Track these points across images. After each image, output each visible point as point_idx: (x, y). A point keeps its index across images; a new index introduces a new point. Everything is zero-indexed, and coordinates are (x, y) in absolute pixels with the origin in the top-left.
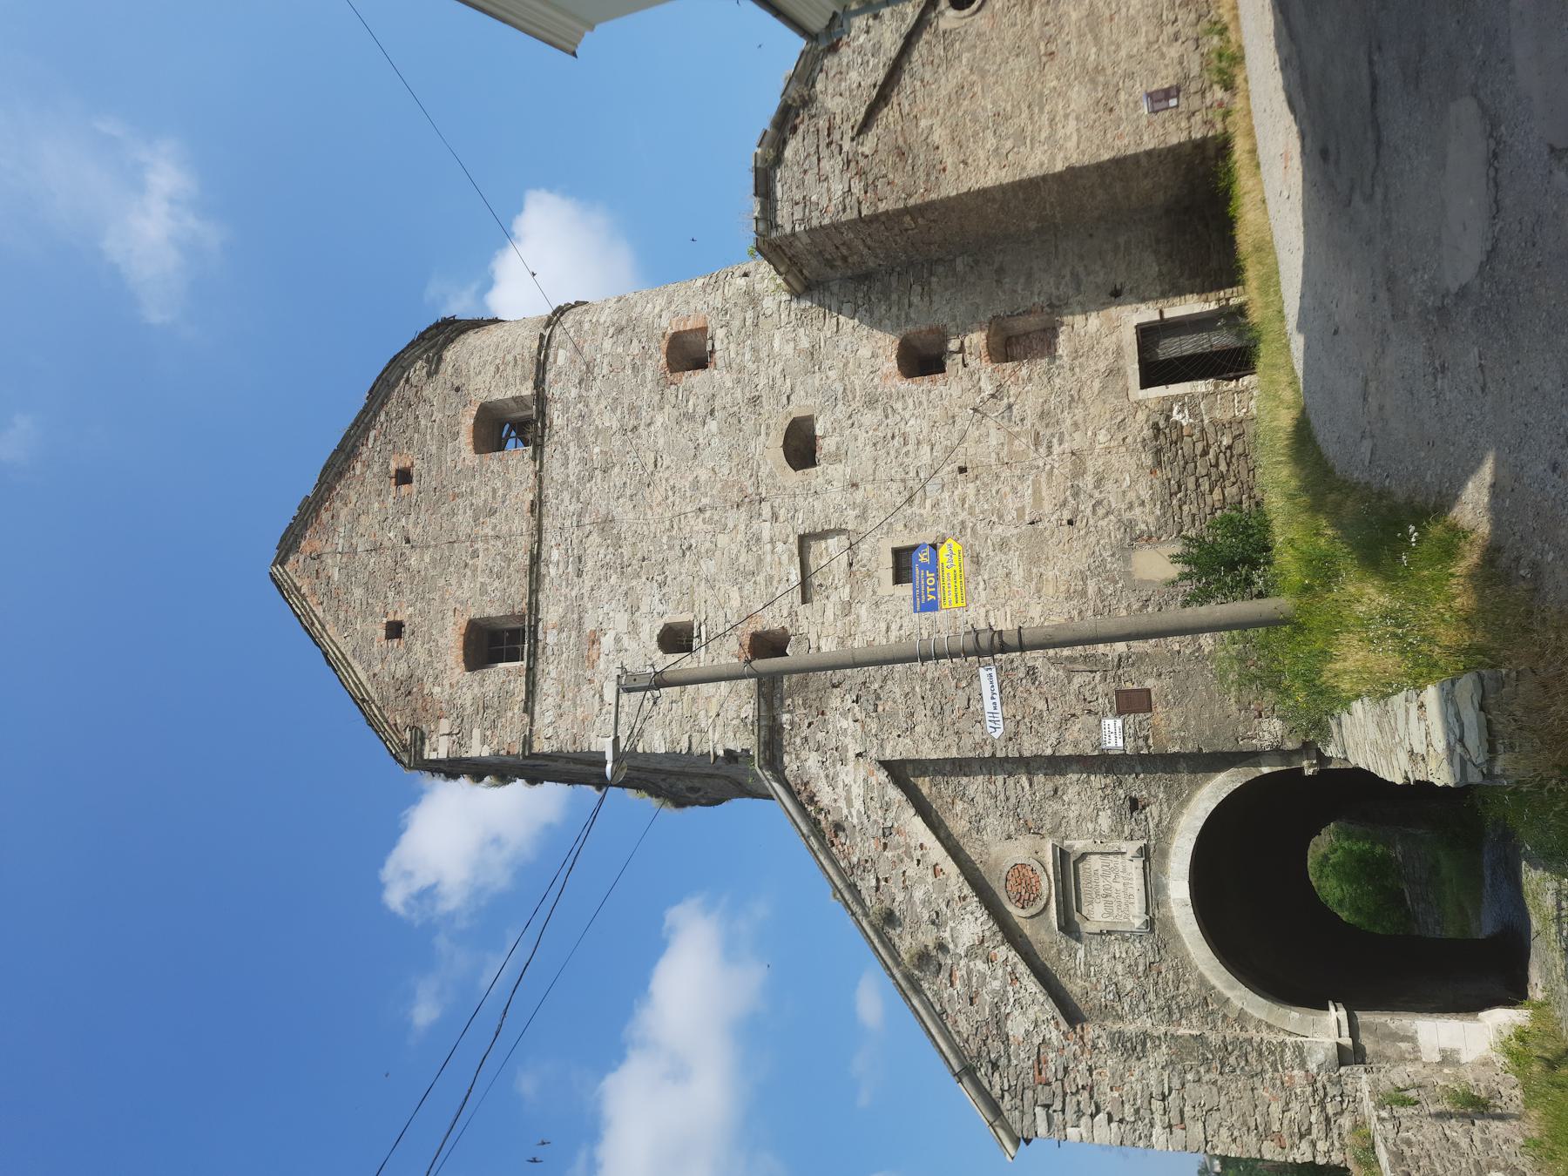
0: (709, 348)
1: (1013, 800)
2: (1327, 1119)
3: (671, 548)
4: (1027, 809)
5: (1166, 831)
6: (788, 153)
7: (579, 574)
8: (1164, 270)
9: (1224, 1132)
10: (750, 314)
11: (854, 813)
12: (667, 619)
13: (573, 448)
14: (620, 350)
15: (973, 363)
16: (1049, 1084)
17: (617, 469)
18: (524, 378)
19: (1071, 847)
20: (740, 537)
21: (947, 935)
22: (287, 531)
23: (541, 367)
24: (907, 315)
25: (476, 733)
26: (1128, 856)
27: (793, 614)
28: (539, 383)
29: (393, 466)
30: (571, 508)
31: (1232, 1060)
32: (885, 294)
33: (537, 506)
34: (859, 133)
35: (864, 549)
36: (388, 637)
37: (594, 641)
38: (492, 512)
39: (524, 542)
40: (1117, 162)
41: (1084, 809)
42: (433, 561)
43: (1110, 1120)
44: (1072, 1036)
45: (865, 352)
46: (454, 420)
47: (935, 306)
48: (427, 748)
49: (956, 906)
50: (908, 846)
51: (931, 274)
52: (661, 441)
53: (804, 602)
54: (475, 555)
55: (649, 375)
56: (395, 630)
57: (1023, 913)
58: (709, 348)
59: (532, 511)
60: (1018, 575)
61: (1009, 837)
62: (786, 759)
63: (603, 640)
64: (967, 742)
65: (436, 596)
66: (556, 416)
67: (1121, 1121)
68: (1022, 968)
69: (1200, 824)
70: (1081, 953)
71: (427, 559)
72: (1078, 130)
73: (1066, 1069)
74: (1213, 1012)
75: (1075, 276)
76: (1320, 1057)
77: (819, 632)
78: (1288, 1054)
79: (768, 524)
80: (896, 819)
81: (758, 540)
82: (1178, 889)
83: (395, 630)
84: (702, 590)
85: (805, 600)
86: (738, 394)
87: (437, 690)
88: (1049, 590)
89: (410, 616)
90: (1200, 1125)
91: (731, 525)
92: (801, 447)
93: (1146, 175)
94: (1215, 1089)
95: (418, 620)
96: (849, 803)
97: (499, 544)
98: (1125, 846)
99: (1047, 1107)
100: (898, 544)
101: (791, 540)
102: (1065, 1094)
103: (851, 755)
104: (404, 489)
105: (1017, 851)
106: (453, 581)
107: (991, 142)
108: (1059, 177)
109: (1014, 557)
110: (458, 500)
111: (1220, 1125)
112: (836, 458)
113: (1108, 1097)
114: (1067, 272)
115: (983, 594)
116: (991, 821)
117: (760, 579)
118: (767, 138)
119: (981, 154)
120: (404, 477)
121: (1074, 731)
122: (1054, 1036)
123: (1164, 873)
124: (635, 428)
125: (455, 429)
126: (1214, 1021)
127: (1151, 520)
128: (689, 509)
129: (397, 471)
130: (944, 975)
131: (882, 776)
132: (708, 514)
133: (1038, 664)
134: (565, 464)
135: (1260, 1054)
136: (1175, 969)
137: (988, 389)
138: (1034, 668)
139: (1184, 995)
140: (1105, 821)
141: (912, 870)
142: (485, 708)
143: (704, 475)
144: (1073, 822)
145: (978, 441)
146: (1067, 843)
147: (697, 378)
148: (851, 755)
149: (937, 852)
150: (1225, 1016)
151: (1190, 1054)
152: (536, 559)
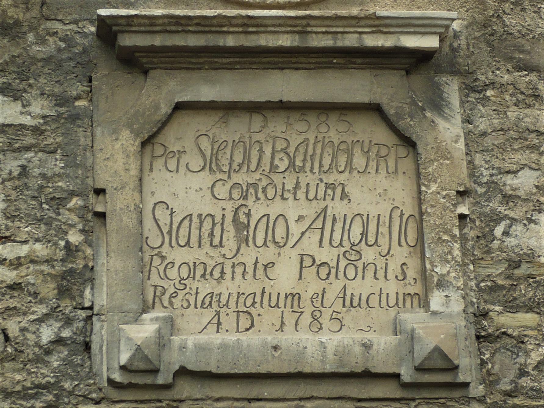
19: (438, 104)
26: (413, 319)
146: (452, 90)
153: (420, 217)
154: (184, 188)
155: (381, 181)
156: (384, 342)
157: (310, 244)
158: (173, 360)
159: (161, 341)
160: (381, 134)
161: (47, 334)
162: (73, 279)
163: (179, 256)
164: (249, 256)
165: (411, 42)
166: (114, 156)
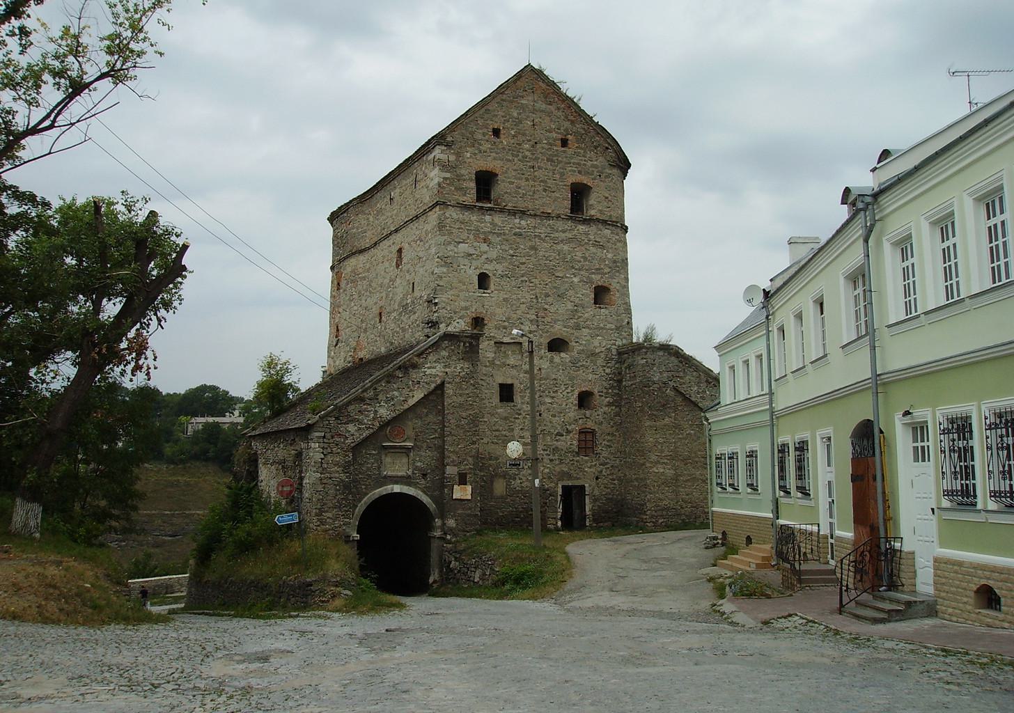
1: (427, 431)
2: (326, 531)
5: (415, 485)
6: (673, 358)
7: (515, 234)
8: (602, 497)
9: (321, 497)
10: (614, 327)
11: (426, 370)
15: (580, 421)
17: (557, 257)
21: (382, 404)
23: (604, 222)
24: (602, 396)
25: (448, 175)
28: (598, 220)
29: (569, 137)
30: (542, 231)
32: (612, 387)
33: (548, 216)
34: (675, 389)
35: (514, 372)
37: (485, 241)
38: (545, 190)
40: (646, 486)
41: (425, 458)
43: (322, 459)
44: (350, 448)
45: (590, 377)
46: (587, 173)
47: (604, 408)
48: (443, 148)
49: (392, 408)
50: (414, 391)
51: (616, 407)
52: (566, 280)
53: (495, 343)
54: (527, 180)
57: (388, 432)
58: (602, 306)
59: (543, 212)
60: (497, 433)
62: (446, 342)
66: (582, 228)
67: (322, 463)
68: (372, 431)
69: (419, 498)
70: (374, 452)
71: (527, 153)
72: (658, 472)
73: (337, 445)
75: (607, 463)
78: (346, 520)
80: (423, 386)
81: (522, 323)
82: (397, 488)
83: (496, 132)
84: (503, 295)
85: (495, 343)
87: (468, 155)
88: (493, 446)
89: (502, 142)
92: (557, 345)
93: (638, 494)
95: (500, 146)
96: (429, 368)
97: (531, 193)
99: (324, 437)
100: (515, 386)
102: (330, 443)
103: (447, 370)
105: (409, 432)
106: (515, 167)
107: (661, 440)
108: (643, 464)
109: (504, 433)
112: (551, 362)
113: (329, 458)
114: (608, 460)
118: (680, 351)
119: (658, 436)
120: (564, 143)
122: (348, 441)
123: (402, 484)
124: (573, 267)
127: (515, 486)
128: (538, 291)
130: (368, 401)
131: (439, 382)
132: (534, 300)
134: (564, 231)
135: (347, 511)
136: (370, 485)
137: (570, 428)
140: (419, 464)
141: (405, 391)
143: (550, 299)
145: (551, 422)
148: (447, 370)
149: (411, 402)
152: (523, 213)
154: (388, 460)
156: (405, 474)
162: (379, 468)
166: (383, 457)
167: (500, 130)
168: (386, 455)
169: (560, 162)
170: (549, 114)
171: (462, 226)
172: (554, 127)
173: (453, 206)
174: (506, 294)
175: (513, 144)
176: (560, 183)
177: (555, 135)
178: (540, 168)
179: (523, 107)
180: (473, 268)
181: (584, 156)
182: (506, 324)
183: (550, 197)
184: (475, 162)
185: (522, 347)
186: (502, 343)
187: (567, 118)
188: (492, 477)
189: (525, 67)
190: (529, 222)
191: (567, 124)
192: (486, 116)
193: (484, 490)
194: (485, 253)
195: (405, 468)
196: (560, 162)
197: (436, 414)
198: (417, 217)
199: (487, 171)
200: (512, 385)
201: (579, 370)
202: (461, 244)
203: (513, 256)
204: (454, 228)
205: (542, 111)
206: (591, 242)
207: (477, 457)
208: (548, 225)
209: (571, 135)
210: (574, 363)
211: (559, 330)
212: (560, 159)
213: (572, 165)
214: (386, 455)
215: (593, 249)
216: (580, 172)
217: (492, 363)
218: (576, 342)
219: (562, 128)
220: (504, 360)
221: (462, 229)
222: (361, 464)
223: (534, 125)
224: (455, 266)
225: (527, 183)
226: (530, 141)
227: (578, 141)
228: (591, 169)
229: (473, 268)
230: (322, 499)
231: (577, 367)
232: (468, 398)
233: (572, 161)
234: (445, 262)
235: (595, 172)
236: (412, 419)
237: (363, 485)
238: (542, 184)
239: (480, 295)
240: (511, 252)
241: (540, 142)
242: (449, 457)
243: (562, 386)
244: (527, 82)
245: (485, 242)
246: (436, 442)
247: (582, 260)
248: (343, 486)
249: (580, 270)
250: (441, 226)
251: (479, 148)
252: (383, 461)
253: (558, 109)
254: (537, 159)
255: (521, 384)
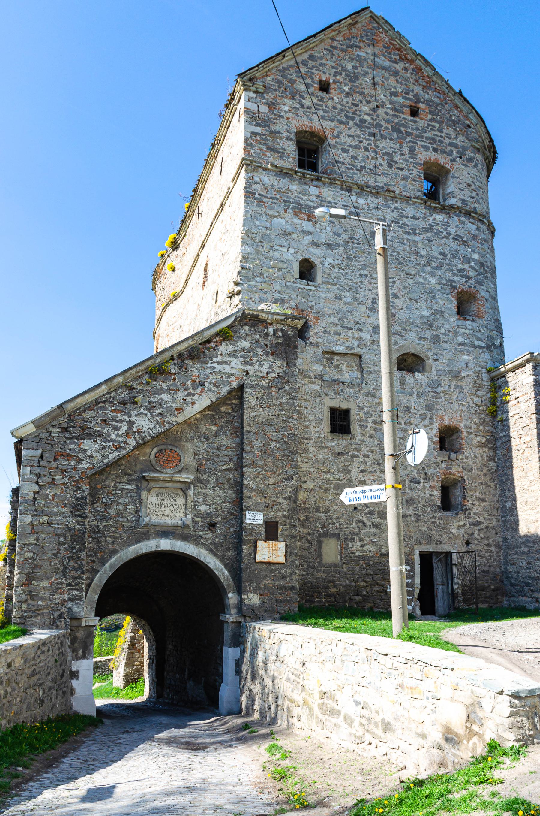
0: (468, 317)
3: (361, 275)
4: (211, 466)
9: (30, 555)
12: (319, 266)
13: (421, 224)
14: (472, 263)
16: (55, 459)
17: (408, 249)
18: (463, 201)
19: (190, 488)
20: (363, 320)
22: (391, 26)
27: (316, 345)
29: (422, 106)
31: (72, 563)
36: (321, 81)
38: (390, 166)
39: (371, 183)
41: (215, 498)
42: (365, 121)
46: (443, 152)
54: (366, 149)
55: (456, 279)
56: (325, 87)
58: (468, 317)
61: (195, 455)
63: (311, 223)
64: (253, 438)
65: (344, 119)
66: (439, 217)
71: (366, 117)
74: (96, 556)
76: (76, 609)
77: (307, 358)
79: (369, 337)
81: (361, 330)
83: (325, 87)
86: (443, 331)
89: (332, 99)
90: (34, 542)
91: (370, 314)
94: (55, 552)
98: (189, 517)
101: (360, 350)
104: (407, 110)
105: (188, 459)
106: (351, 132)
110: (398, 144)
111: (34, 553)
112: (402, 383)
115: (320, 457)
116: (205, 446)
117: (339, 328)
121: (257, 498)
125: (439, 151)
126: (91, 556)
129: (419, 108)
133: (294, 482)
134: (415, 218)
138: (292, 479)
139: (106, 541)
140: (203, 508)
142: (274, 138)
144: (203, 491)
146: (192, 486)
147: (453, 305)
150: (94, 562)
151: (75, 540)
153: (186, 505)
155: (181, 499)
156: (180, 523)
157: (171, 508)
158: (151, 523)
159: (150, 521)
160: (182, 493)
161: (133, 519)
162: (137, 511)
163: (152, 509)
164: (162, 509)
165: (187, 480)
166: (144, 494)
167: (329, 84)
168: (149, 491)
169: (409, 134)
170: (396, 73)
171: (278, 196)
172: (400, 90)
173: (265, 169)
174: (339, 289)
175: (347, 103)
176: (411, 160)
177: (401, 100)
178: (383, 137)
179: (361, 60)
180: (292, 251)
181: (440, 131)
182: (339, 328)
183: (396, 174)
184: (293, 120)
185: (361, 361)
186: (334, 353)
187: (417, 81)
188: (320, 535)
189: (363, 10)
190: (369, 201)
191: (418, 89)
192: (311, 63)
193: (306, 551)
194: (310, 233)
195: (180, 513)
196: (409, 134)
197: (232, 434)
198: (222, 206)
199: (312, 134)
200: (347, 412)
201: (440, 398)
202: (275, 219)
203: (348, 242)
204: (267, 197)
205: (386, 69)
206: (452, 237)
207: (293, 499)
208: (395, 208)
209: (423, 103)
210: (433, 386)
211: (412, 343)
212: (410, 130)
213: (424, 139)
214: (149, 491)
215: (454, 245)
216: (435, 150)
217: (320, 377)
218: (436, 360)
219: (411, 93)
220: (336, 377)
221: (277, 199)
222: (106, 504)
223: (374, 84)
224: (267, 246)
225: (367, 153)
226: (369, 102)
227: (431, 112)
228: (449, 148)
229: (292, 251)
230: (33, 559)
231: (436, 393)
232: (281, 410)
233: (425, 135)
234: (252, 239)
235: (454, 152)
236: (193, 438)
237: (110, 537)
238: (386, 158)
239: (302, 286)
240: (345, 237)
241: (383, 106)
242: (250, 498)
243: (418, 416)
244: (364, 31)
245: (309, 220)
246: (231, 476)
247: (441, 257)
248: (71, 536)
249: (439, 268)
250: (249, 193)
251: (300, 101)
252: (145, 501)
253: (406, 69)
254: (379, 126)
255: (361, 409)
